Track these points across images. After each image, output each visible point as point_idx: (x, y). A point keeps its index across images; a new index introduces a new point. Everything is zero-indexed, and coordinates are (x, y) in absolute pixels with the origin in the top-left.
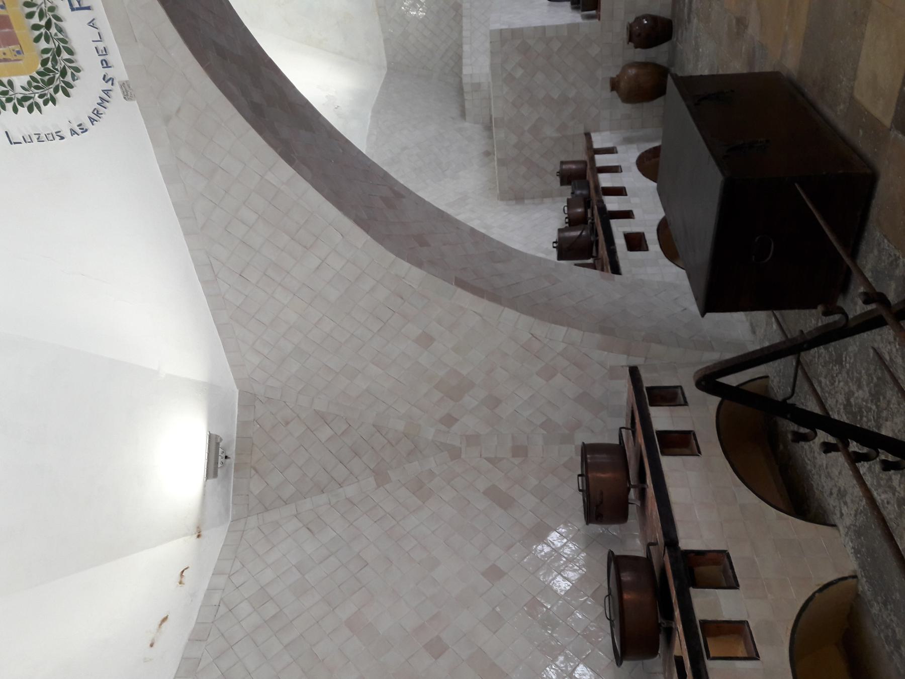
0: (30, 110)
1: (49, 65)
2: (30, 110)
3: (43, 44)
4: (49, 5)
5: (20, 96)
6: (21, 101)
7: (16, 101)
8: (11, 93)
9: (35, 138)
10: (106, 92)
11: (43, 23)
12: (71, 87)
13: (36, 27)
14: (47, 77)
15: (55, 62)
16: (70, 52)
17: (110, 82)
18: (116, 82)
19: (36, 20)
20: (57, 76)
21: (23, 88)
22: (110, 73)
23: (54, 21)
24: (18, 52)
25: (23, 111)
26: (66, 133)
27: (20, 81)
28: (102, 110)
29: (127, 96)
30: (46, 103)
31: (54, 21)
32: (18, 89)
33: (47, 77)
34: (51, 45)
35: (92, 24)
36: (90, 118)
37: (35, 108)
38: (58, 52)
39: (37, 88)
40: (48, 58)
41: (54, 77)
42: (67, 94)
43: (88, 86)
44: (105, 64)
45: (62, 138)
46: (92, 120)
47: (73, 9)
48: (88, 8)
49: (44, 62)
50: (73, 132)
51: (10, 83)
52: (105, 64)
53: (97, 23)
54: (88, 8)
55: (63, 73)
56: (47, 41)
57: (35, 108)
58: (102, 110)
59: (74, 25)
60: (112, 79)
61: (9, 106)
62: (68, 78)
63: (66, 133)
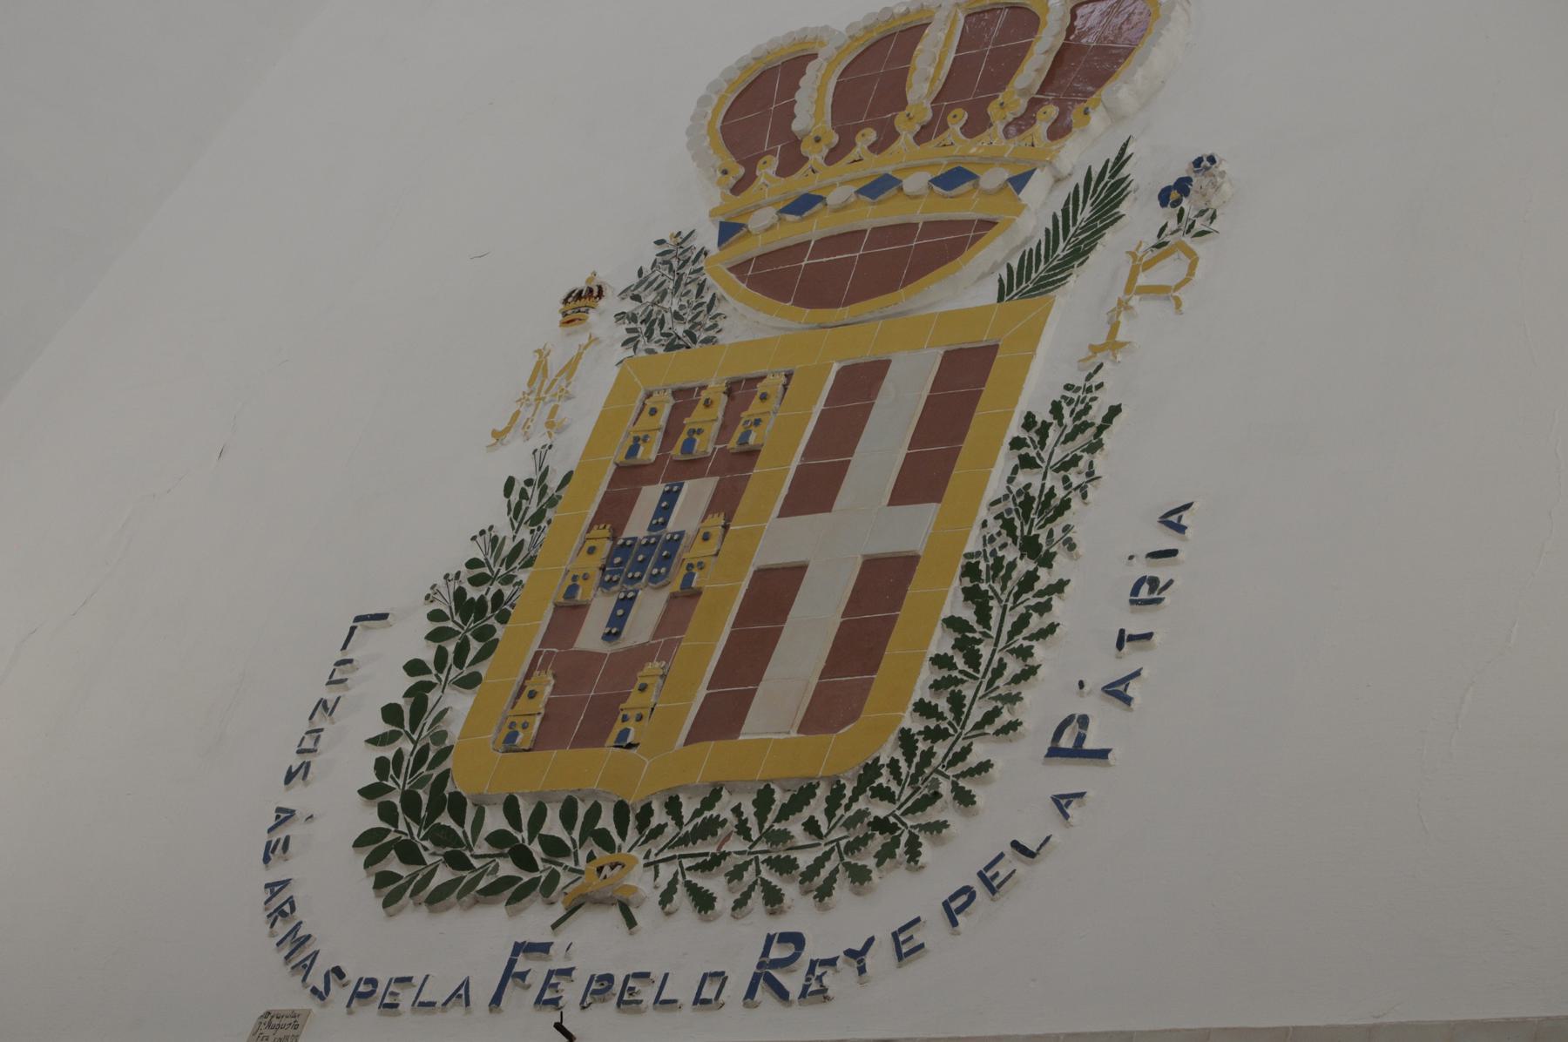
1: (445, 820)
3: (495, 821)
4: (565, 879)
6: (418, 694)
7: (432, 678)
8: (455, 671)
13: (539, 816)
14: (425, 798)
15: (442, 837)
16: (437, 899)
17: (321, 988)
18: (311, 1004)
19: (553, 826)
20: (415, 832)
23: (526, 877)
24: (512, 737)
26: (292, 798)
28: (282, 928)
31: (526, 877)
33: (425, 798)
35: (462, 994)
37: (388, 728)
38: (457, 861)
39: (421, 757)
40: (461, 823)
41: (417, 820)
43: (348, 916)
45: (290, 776)
47: (519, 948)
48: (496, 1000)
49: (457, 806)
51: (470, 682)
52: (364, 992)
53: (457, 1011)
54: (496, 1000)
55: (409, 853)
56: (497, 839)
57: (388, 728)
58: (282, 928)
59: (478, 937)
62: (393, 864)
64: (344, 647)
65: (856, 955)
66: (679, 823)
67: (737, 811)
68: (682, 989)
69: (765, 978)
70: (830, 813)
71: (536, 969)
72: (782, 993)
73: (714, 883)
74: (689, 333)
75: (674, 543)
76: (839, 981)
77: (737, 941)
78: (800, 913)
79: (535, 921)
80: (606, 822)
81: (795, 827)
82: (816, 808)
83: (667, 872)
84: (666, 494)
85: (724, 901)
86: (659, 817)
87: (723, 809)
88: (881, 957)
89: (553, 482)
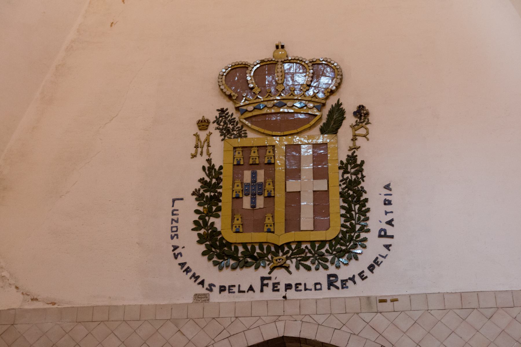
0: (195, 222)
2: (195, 222)
5: (207, 218)
9: (175, 217)
10: (202, 283)
11: (255, 254)
12: (210, 259)
21: (213, 223)
22: (216, 289)
25: (196, 217)
26: (175, 242)
27: (218, 223)
28: (190, 274)
29: (197, 297)
30: (199, 235)
32: (212, 220)
34: (240, 255)
35: (251, 289)
36: (185, 263)
42: (204, 254)
44: (222, 289)
45: (172, 238)
46: (182, 265)
50: (175, 248)
51: (218, 216)
52: (222, 289)
54: (262, 291)
59: (250, 276)
60: (211, 290)
61: (201, 209)
63: (175, 242)
64: (173, 206)
65: (352, 279)
66: (293, 250)
67: (306, 247)
68: (310, 286)
69: (331, 284)
70: (331, 248)
71: (270, 282)
72: (337, 288)
73: (308, 263)
74: (239, 133)
75: (261, 184)
76: (350, 283)
77: (321, 276)
78: (332, 270)
79: (264, 272)
80: (273, 249)
81: (323, 251)
82: (327, 246)
83: (294, 260)
84: (252, 173)
85: (313, 267)
86: (286, 249)
87: (303, 246)
88: (357, 279)
89: (217, 167)
